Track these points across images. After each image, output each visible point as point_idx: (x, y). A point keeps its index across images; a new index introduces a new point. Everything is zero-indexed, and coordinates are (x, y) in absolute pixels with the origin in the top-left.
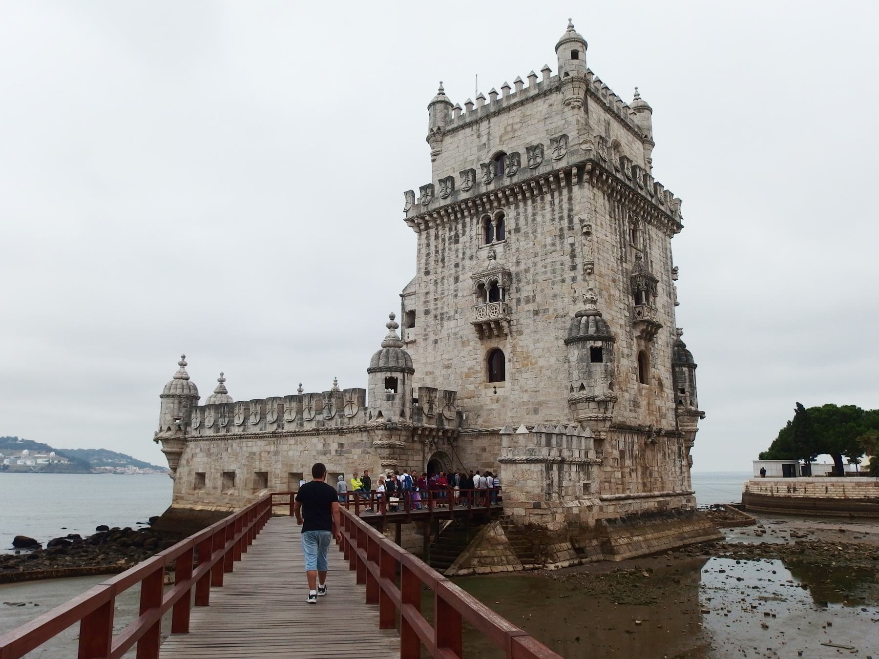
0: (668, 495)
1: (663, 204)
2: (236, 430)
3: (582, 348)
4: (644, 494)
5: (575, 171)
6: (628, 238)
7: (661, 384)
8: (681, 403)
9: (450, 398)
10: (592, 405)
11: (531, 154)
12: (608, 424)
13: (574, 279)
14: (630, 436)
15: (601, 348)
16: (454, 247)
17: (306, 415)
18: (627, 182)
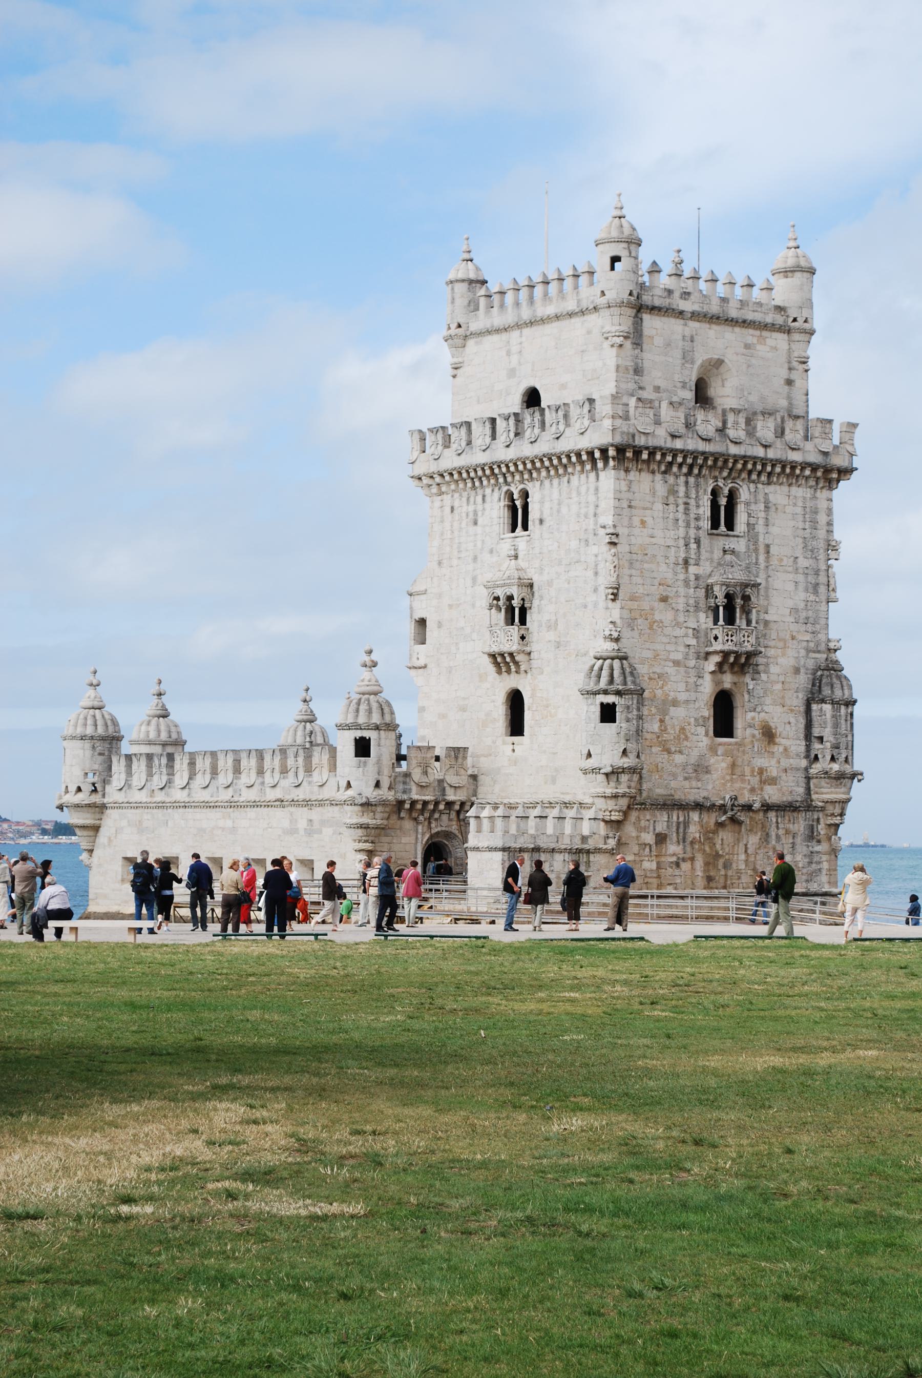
2: (179, 795)
3: (592, 704)
4: (705, 892)
5: (597, 454)
6: (706, 524)
7: (769, 735)
8: (816, 758)
9: (456, 758)
10: (601, 778)
11: (554, 414)
12: (624, 802)
13: (596, 605)
14: (681, 813)
15: (614, 703)
16: (472, 529)
17: (268, 779)
18: (702, 446)
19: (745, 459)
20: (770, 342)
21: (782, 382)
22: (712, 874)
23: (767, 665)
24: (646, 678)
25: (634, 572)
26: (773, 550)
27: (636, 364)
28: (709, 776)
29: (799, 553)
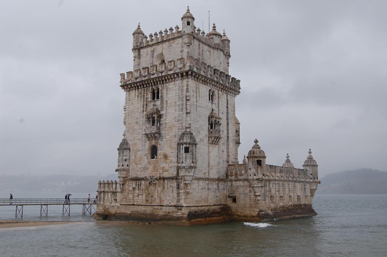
0: (162, 206)
1: (172, 70)
4: (144, 204)
6: (149, 99)
7: (166, 157)
19: (155, 78)
20: (176, 42)
21: (180, 52)
22: (148, 199)
23: (165, 136)
24: (131, 144)
25: (129, 117)
26: (168, 102)
27: (138, 63)
28: (147, 170)
29: (177, 100)
